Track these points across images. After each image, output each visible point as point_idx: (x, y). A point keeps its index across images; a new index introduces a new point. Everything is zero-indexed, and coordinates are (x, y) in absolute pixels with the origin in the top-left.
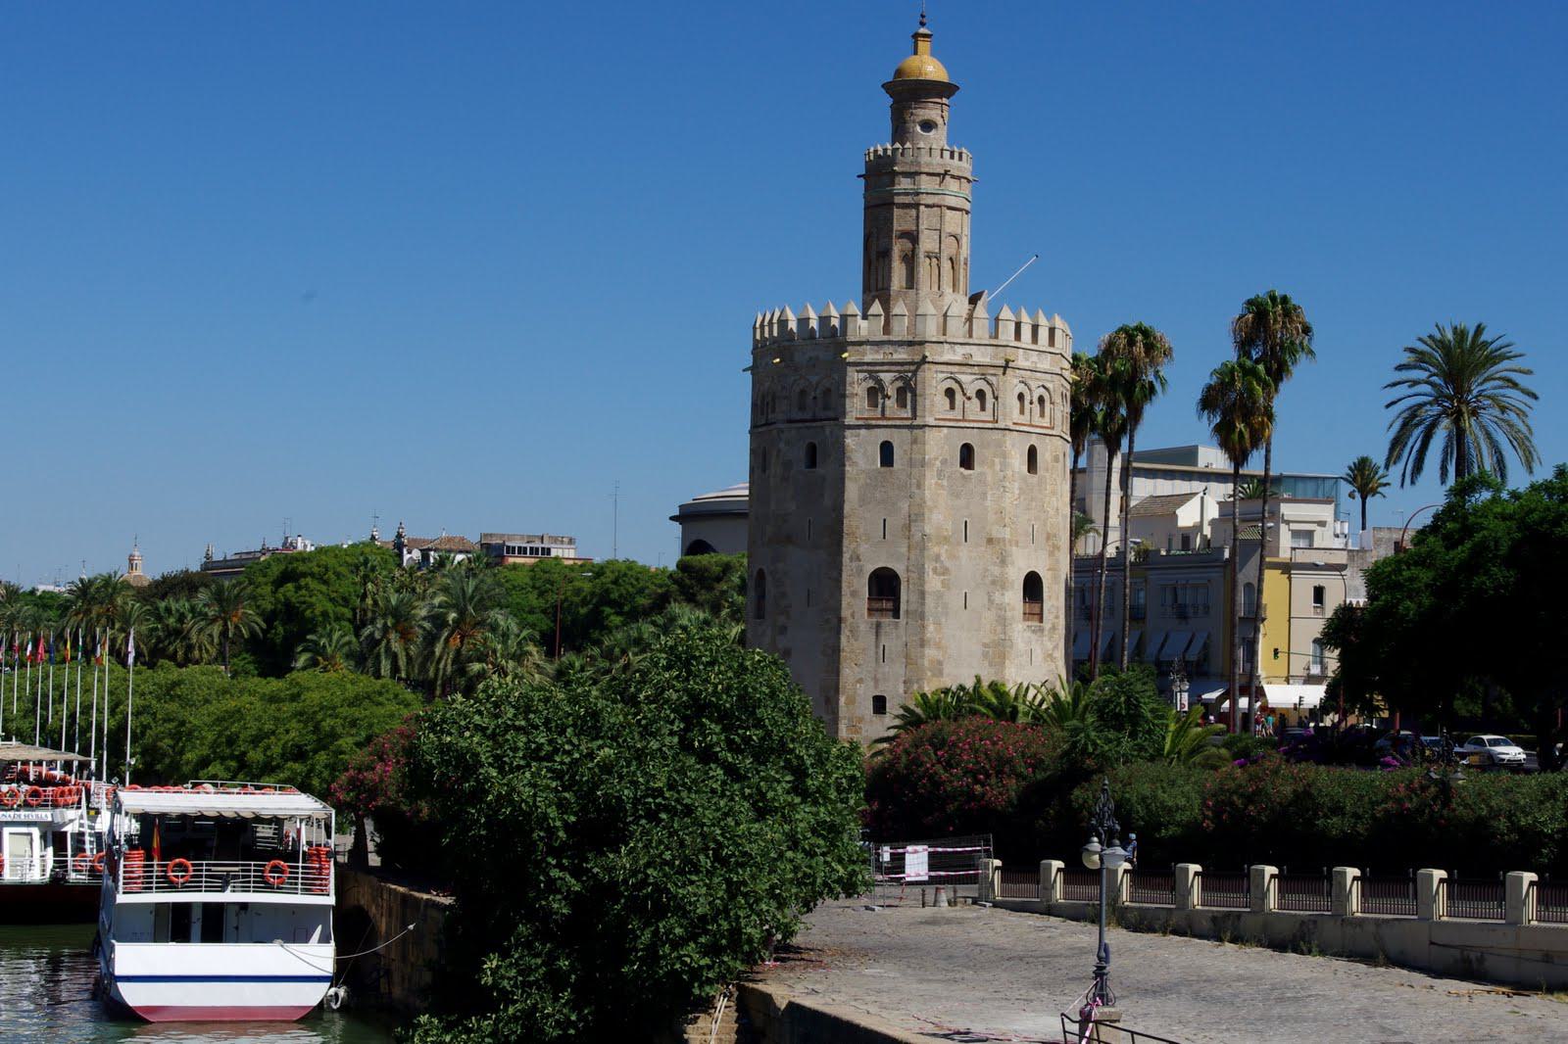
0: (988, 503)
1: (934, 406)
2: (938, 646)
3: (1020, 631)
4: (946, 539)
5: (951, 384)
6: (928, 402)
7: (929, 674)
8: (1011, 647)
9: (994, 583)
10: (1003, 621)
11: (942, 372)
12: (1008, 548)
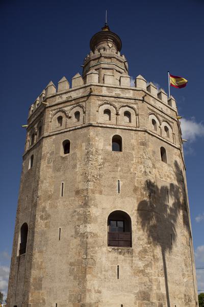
0: (77, 170)
1: (51, 123)
2: (40, 268)
3: (105, 255)
4: (50, 197)
5: (60, 114)
6: (46, 126)
7: (33, 287)
8: (95, 263)
9: (78, 219)
10: (85, 247)
11: (55, 110)
12: (90, 194)
